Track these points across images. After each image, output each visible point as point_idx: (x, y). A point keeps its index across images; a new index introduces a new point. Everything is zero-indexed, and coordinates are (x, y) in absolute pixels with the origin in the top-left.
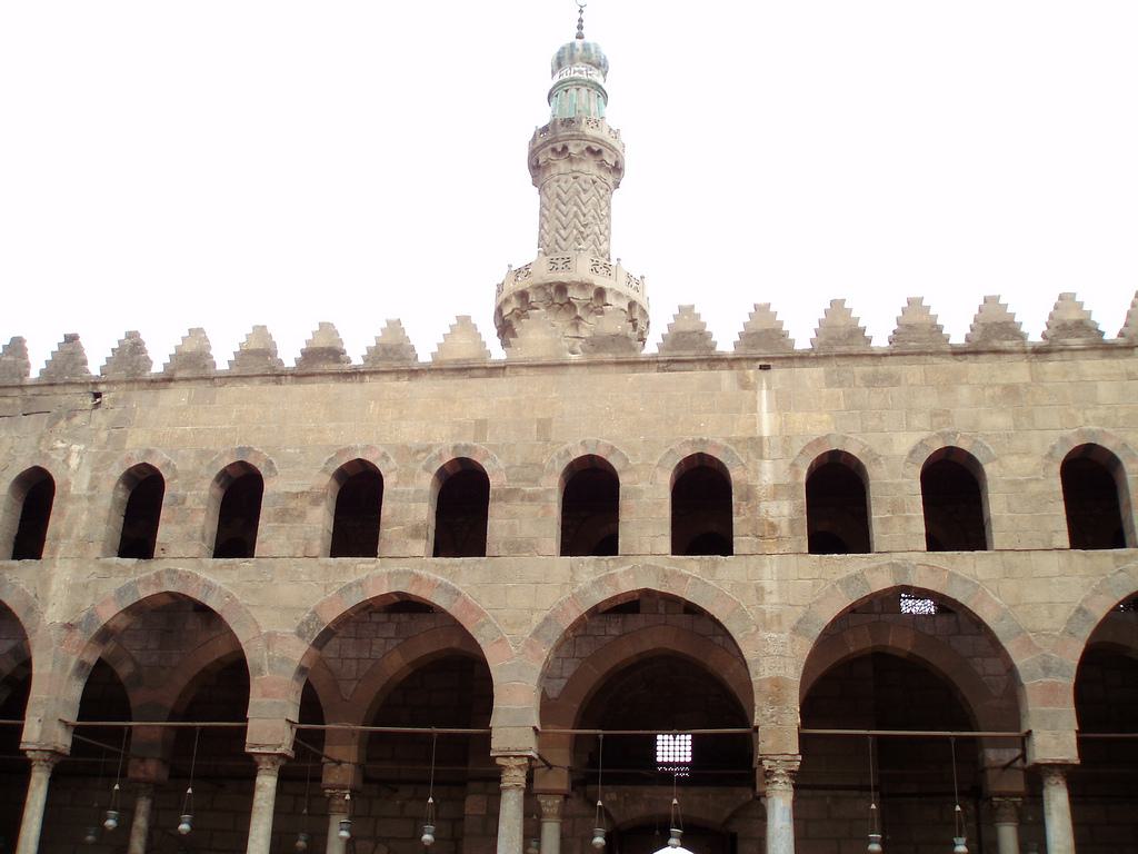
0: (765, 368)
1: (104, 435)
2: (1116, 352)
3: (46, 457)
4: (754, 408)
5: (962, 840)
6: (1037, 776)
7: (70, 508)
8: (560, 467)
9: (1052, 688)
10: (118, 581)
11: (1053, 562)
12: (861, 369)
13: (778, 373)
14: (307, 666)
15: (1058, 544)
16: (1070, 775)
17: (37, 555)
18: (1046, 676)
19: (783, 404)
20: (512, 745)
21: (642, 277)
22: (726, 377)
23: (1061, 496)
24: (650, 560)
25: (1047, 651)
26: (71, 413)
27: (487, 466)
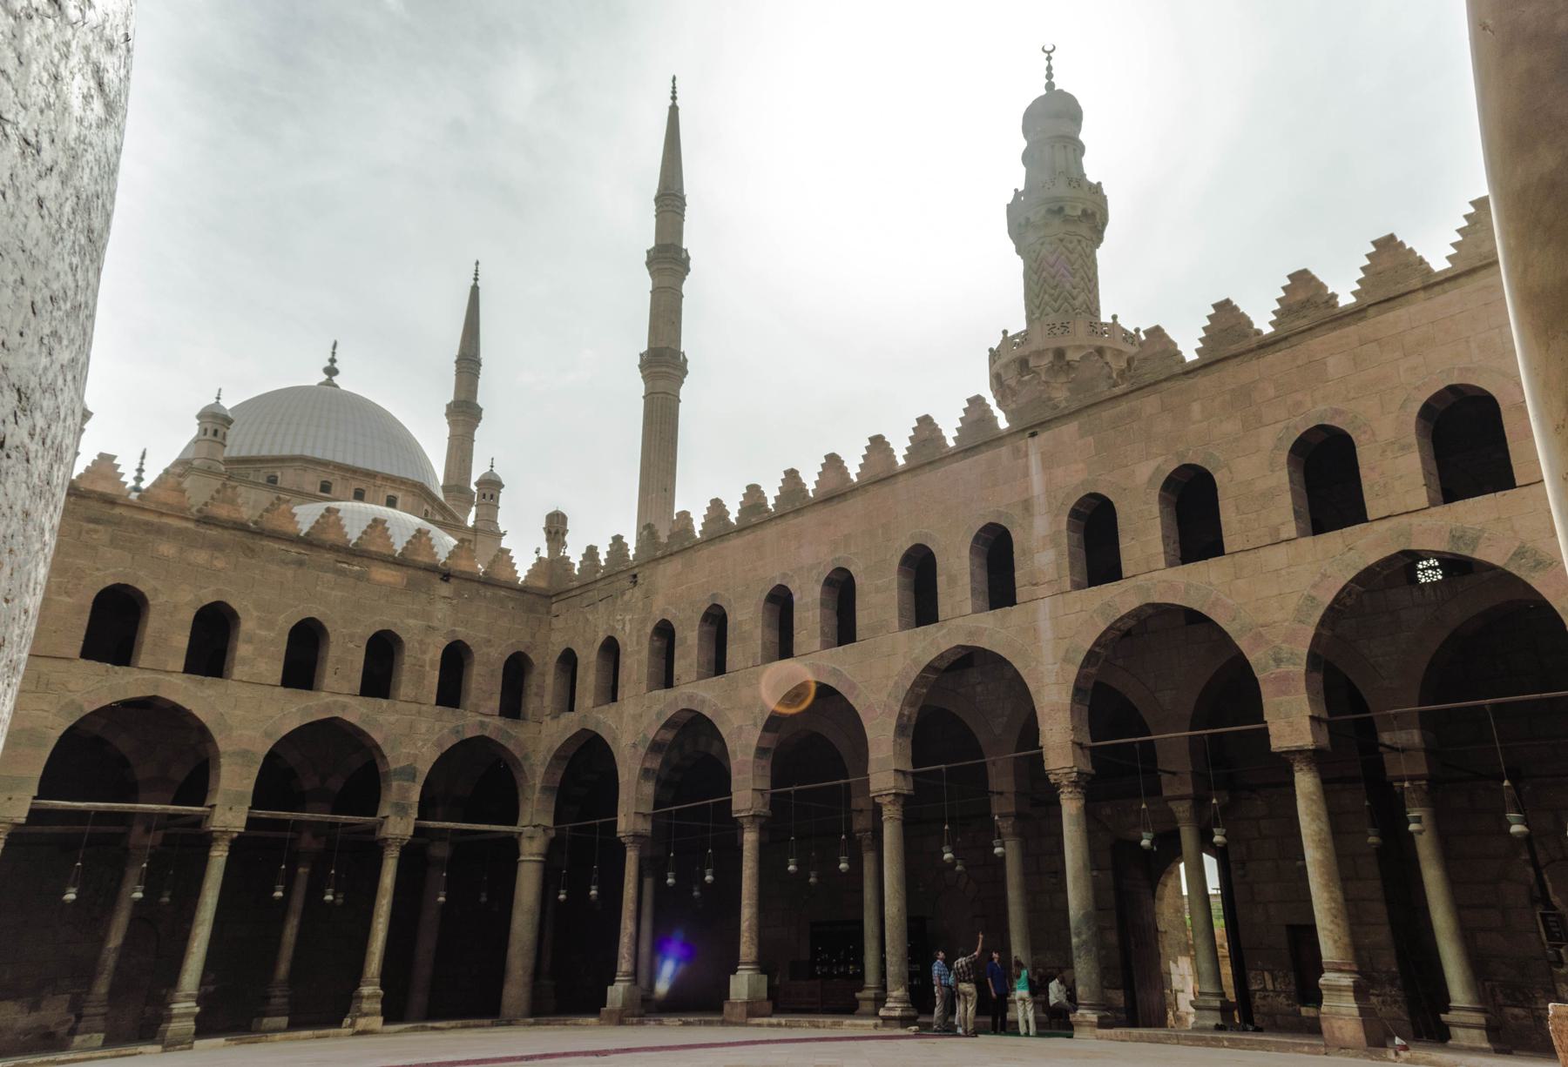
0: (1033, 435)
1: (640, 604)
2: (1347, 320)
3: (614, 628)
4: (1026, 474)
5: (1150, 835)
6: (1283, 765)
7: (628, 662)
8: (896, 561)
9: (1286, 678)
10: (656, 708)
11: (1279, 556)
12: (1107, 413)
13: (1044, 437)
14: (765, 745)
15: (1284, 536)
16: (1316, 758)
17: (614, 699)
18: (1278, 666)
19: (1048, 462)
20: (882, 786)
21: (1114, 317)
22: (1004, 451)
23: (1288, 486)
24: (959, 621)
25: (1278, 642)
26: (623, 594)
27: (852, 570)
